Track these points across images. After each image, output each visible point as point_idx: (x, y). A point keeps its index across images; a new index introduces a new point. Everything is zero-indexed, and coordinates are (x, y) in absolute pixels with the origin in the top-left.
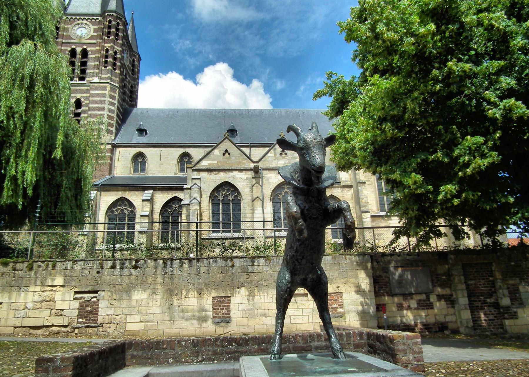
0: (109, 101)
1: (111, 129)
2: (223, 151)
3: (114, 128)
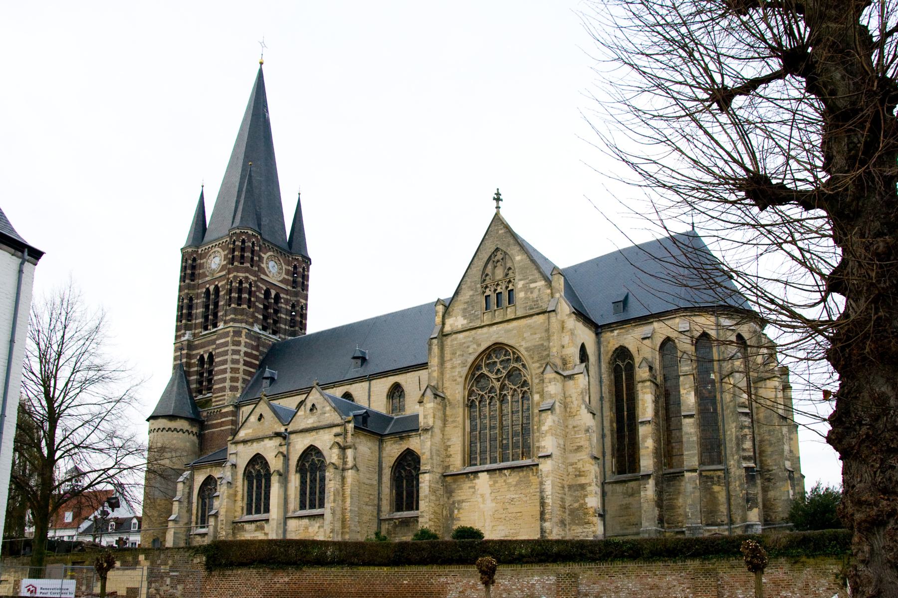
0: (233, 350)
1: (235, 384)
2: (258, 416)
3: (241, 381)
